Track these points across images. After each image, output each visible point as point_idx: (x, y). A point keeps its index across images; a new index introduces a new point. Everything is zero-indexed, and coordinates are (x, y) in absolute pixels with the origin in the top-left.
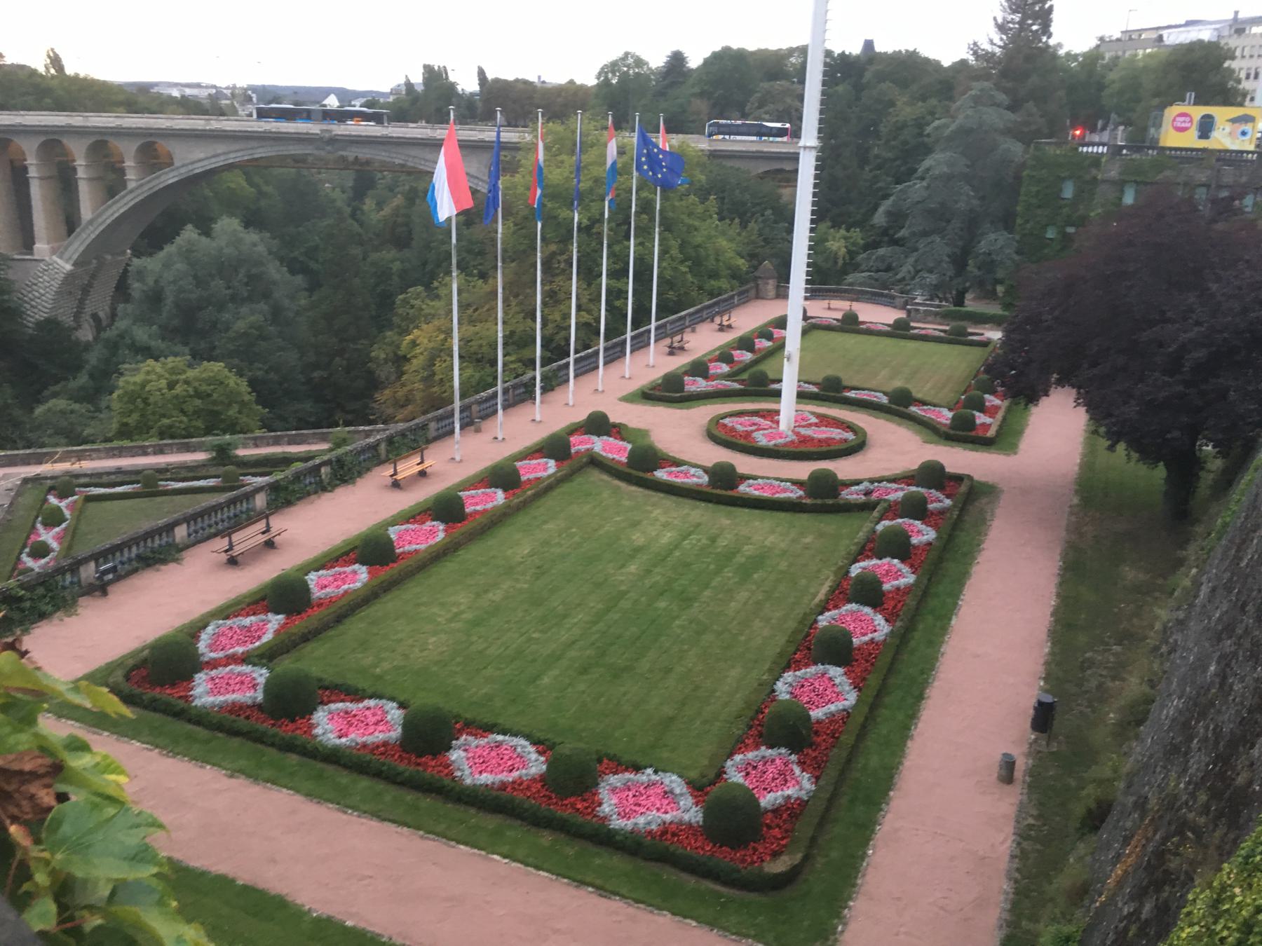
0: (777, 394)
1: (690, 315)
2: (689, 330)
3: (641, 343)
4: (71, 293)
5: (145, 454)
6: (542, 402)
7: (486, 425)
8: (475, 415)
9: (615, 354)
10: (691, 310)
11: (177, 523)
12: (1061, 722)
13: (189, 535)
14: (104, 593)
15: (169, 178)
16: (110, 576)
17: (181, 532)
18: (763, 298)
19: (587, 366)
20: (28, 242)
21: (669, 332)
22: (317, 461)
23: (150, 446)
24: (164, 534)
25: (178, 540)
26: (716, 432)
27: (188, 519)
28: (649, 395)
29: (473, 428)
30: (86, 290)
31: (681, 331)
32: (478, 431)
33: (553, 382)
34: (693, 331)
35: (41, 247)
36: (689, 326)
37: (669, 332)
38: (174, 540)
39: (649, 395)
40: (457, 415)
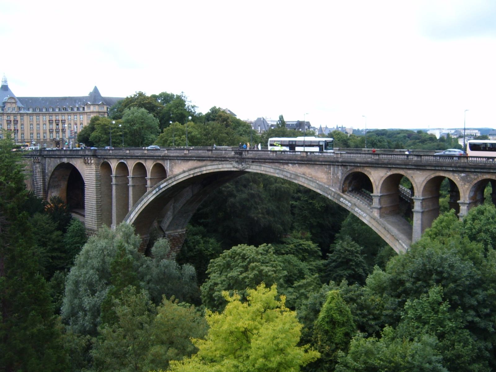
15: (164, 185)
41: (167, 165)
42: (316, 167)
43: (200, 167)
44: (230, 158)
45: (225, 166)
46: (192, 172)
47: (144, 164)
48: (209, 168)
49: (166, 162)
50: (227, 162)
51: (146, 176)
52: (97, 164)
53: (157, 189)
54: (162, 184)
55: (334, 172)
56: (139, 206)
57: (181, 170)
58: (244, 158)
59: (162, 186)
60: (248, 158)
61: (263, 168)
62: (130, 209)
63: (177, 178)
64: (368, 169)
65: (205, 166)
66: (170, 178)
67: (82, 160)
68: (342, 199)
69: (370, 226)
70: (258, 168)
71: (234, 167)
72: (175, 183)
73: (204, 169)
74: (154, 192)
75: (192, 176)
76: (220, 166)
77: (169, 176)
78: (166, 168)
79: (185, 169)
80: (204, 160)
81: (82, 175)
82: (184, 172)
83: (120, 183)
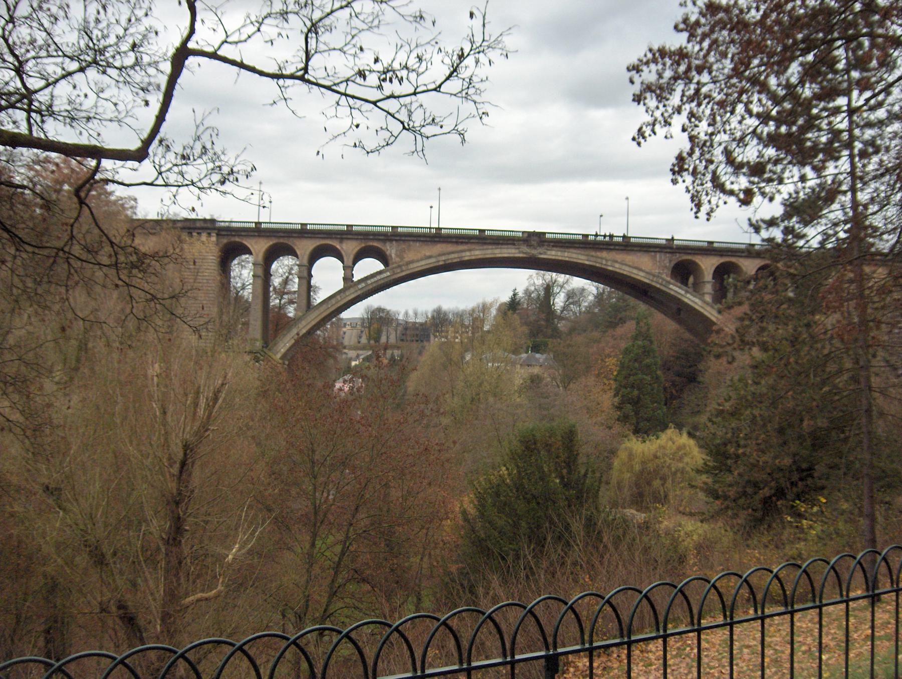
45: (505, 251)
46: (444, 258)
47: (338, 247)
48: (477, 253)
49: (388, 245)
55: (661, 258)
57: (419, 256)
61: (566, 254)
63: (415, 265)
64: (699, 257)
65: (470, 250)
68: (671, 286)
69: (702, 310)
70: (559, 253)
71: (520, 253)
73: (468, 254)
75: (441, 263)
76: (497, 251)
78: (388, 253)
79: (428, 254)
80: (467, 243)
82: (430, 257)
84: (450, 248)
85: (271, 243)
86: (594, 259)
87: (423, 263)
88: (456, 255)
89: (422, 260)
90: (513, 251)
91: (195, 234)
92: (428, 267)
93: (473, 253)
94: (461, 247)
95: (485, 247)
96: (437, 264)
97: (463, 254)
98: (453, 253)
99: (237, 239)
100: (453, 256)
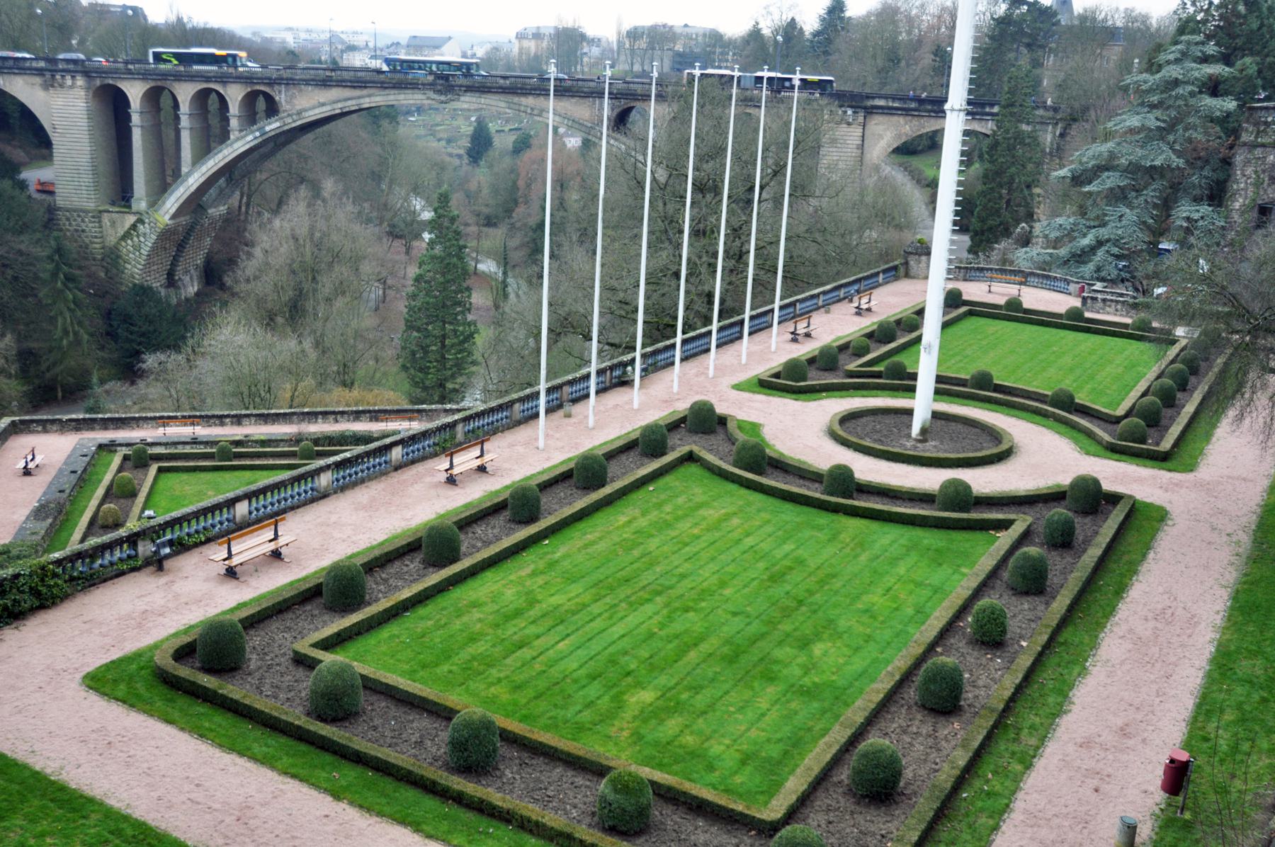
0: (911, 390)
1: (824, 293)
2: (823, 310)
3: (761, 325)
4: (165, 249)
5: (222, 424)
6: (641, 387)
7: (577, 409)
8: (565, 397)
9: (730, 336)
10: (828, 287)
11: (237, 499)
12: (1199, 782)
13: (250, 513)
14: (160, 568)
15: (272, 126)
16: (167, 550)
17: (242, 509)
18: (913, 278)
19: (696, 350)
20: (122, 194)
21: (798, 312)
22: (388, 441)
23: (228, 416)
24: (225, 510)
25: (238, 519)
26: (837, 428)
27: (249, 496)
28: (768, 385)
29: (561, 413)
30: (181, 247)
31: (807, 314)
32: (568, 416)
33: (656, 364)
34: (828, 312)
35: (140, 200)
36: (823, 306)
37: (798, 312)
38: (234, 517)
39: (768, 385)
40: (543, 399)
41: (281, 96)
42: (574, 100)
43: (359, 97)
44: (423, 84)
46: (340, 105)
47: (222, 91)
48: (378, 99)
49: (276, 87)
50: (416, 91)
51: (228, 111)
52: (87, 89)
53: (257, 134)
54: (270, 124)
56: (211, 163)
57: (313, 102)
58: (453, 86)
59: (268, 129)
60: (461, 86)
62: (184, 170)
63: (307, 114)
65: (369, 96)
66: (289, 115)
67: (38, 80)
71: (428, 98)
72: (299, 123)
73: (367, 100)
74: (250, 137)
75: (338, 111)
77: (284, 111)
78: (277, 98)
79: (322, 100)
80: (366, 87)
81: (33, 110)
82: (323, 105)
83: (145, 124)
84: (348, 93)
85: (148, 87)
86: (517, 107)
87: (317, 111)
88: (354, 102)
89: (314, 108)
90: (420, 96)
91: (58, 77)
92: (322, 116)
93: (373, 99)
94: (357, 92)
95: (387, 91)
96: (333, 113)
97: (362, 101)
98: (349, 99)
99: (111, 82)
100: (349, 103)
